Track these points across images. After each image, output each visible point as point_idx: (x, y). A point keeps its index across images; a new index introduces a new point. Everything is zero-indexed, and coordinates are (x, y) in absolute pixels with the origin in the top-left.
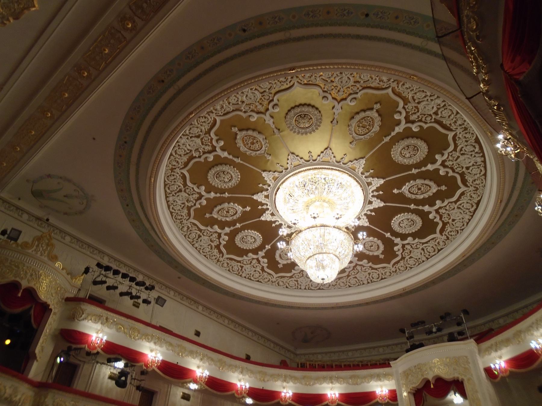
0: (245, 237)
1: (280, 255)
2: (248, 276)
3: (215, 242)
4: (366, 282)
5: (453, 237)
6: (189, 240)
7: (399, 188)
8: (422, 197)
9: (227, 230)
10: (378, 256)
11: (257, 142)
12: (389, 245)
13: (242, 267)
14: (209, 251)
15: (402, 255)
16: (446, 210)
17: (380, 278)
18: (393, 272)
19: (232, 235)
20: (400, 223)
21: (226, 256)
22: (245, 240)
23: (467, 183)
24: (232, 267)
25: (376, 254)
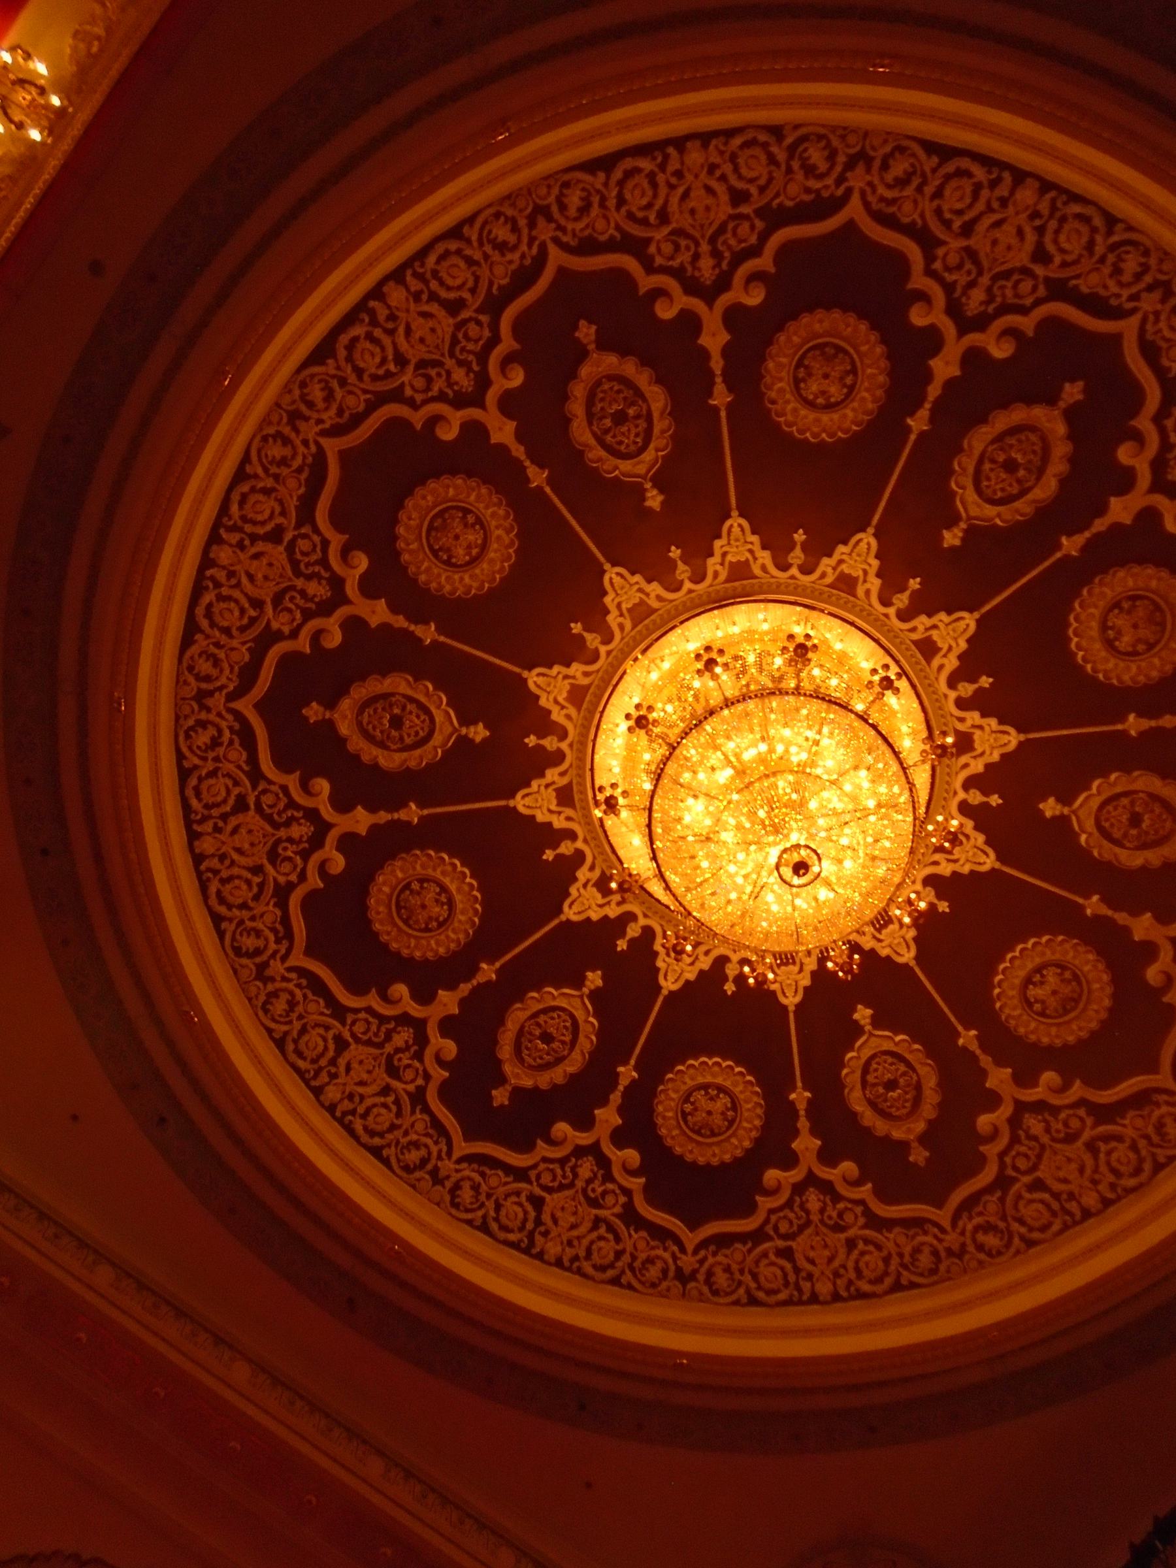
0: (415, 886)
2: (347, 1105)
3: (286, 867)
4: (824, 1288)
6: (194, 803)
7: (1066, 799)
9: (361, 820)
10: (904, 1146)
11: (638, 417)
12: (963, 1090)
14: (244, 906)
15: (1002, 1166)
17: (888, 1281)
18: (950, 1252)
19: (369, 854)
21: (298, 959)
22: (415, 901)
24: (303, 1031)
25: (897, 1134)
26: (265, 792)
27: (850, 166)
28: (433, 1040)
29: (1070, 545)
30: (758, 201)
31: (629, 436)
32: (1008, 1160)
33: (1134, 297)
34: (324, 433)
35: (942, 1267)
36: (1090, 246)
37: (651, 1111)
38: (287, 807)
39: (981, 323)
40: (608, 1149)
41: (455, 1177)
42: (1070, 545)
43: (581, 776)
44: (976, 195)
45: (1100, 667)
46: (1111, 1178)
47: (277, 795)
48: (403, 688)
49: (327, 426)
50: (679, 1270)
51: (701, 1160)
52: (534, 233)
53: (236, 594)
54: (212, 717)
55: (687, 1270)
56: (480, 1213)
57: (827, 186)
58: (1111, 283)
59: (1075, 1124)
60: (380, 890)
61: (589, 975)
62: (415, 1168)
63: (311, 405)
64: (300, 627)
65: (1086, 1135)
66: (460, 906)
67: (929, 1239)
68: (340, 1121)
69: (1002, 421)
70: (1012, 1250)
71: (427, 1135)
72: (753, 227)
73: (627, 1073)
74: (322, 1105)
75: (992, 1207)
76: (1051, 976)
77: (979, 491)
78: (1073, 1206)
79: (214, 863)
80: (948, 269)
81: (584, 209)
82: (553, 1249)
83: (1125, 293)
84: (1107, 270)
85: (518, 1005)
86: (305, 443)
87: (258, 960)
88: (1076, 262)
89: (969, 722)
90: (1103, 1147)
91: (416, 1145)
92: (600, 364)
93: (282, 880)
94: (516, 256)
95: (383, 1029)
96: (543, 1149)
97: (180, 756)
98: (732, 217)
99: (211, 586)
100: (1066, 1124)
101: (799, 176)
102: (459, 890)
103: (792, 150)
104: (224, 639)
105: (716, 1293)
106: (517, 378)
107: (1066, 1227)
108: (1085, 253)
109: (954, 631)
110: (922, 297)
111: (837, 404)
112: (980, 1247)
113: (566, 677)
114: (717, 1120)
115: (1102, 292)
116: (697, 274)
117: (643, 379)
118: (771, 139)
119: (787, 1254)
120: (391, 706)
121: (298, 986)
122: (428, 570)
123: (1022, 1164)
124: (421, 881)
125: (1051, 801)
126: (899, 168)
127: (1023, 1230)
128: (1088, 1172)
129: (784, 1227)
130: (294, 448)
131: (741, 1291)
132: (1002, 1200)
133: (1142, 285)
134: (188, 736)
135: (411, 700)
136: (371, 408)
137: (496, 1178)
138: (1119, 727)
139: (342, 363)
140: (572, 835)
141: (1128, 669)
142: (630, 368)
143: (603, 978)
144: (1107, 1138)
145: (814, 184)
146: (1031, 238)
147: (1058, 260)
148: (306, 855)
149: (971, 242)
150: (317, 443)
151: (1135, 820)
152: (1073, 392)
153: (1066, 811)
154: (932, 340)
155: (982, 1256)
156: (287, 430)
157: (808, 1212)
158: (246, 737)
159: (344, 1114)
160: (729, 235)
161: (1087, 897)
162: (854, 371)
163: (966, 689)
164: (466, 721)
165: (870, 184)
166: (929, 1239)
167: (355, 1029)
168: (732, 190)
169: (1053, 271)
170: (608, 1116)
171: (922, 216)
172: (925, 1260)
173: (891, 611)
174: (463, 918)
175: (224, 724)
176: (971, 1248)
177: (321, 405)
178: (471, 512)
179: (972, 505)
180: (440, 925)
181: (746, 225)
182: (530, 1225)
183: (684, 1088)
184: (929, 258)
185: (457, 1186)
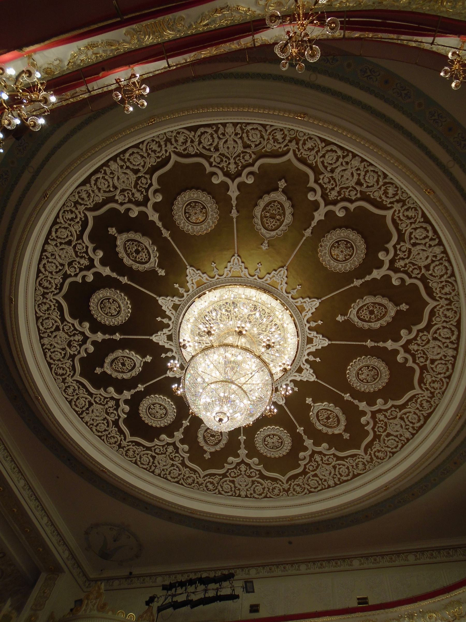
1: (116, 358)
2: (48, 347)
3: (73, 270)
4: (157, 471)
5: (294, 493)
7: (314, 402)
8: (320, 428)
9: (106, 271)
10: (206, 452)
11: (278, 220)
13: (57, 329)
15: (227, 472)
16: (322, 460)
17: (176, 480)
18: (198, 483)
20: (269, 436)
23: (369, 449)
25: (205, 448)
26: (80, 244)
27: (398, 201)
28: (87, 344)
29: (369, 343)
30: (364, 188)
31: (271, 223)
32: (230, 471)
33: (441, 298)
34: (174, 152)
35: (193, 485)
36: (442, 276)
37: (141, 401)
38: (84, 252)
39: (396, 271)
40: (121, 403)
41: (70, 384)
42: (369, 343)
43: (185, 306)
44: (424, 238)
45: (350, 378)
46: (252, 492)
47: (83, 247)
48: (147, 244)
49: (177, 151)
50: (120, 444)
51: (146, 422)
52: (289, 144)
53: (110, 180)
54: (77, 212)
55: (122, 445)
56: (71, 398)
57: (387, 202)
58: (438, 289)
59: (253, 474)
60: (99, 295)
61: (148, 356)
62: (59, 375)
63: (176, 141)
64: (125, 203)
65: (254, 479)
66: (122, 314)
67: (195, 476)
68: (43, 350)
69: (379, 299)
70: (214, 492)
71: (69, 368)
72: (356, 194)
73: (141, 387)
74: (41, 342)
75: (217, 479)
76: (275, 439)
77: (358, 312)
78: (238, 492)
79: (49, 255)
80: (400, 250)
81: (311, 150)
82: (87, 419)
84: (440, 285)
85: (121, 351)
86: (166, 151)
87: (46, 291)
88: (434, 276)
89: (305, 367)
90: (256, 484)
91: (64, 369)
92: (278, 196)
93: (68, 272)
94: (278, 146)
95: (74, 332)
96: (102, 391)
97: (57, 216)
98: (353, 187)
99: (103, 172)
100: (251, 473)
101: (381, 192)
102: (124, 310)
103: (385, 184)
104: (96, 191)
105: (127, 455)
106: (250, 181)
107: (232, 495)
109: (321, 342)
110: (387, 251)
111: (339, 261)
112: (206, 486)
113: (200, 276)
114: (158, 415)
115: (434, 289)
116: (329, 194)
117: (289, 210)
118: (382, 176)
119: (154, 458)
120: (139, 246)
121: (54, 305)
122: (179, 216)
123: (233, 474)
124: (114, 300)
125: (311, 399)
126: (410, 213)
127: (221, 489)
128: (248, 487)
129: (157, 451)
130: (161, 150)
131: (134, 459)
132: (221, 479)
133: (445, 297)
134: (64, 212)
135: (147, 249)
136: (196, 155)
137: (82, 391)
138: (343, 395)
139: (196, 136)
140: (170, 319)
141: (357, 383)
142: (287, 204)
143: (152, 360)
144: (258, 482)
145: (383, 197)
146: (429, 261)
147: (430, 272)
148: (81, 270)
149: (413, 249)
150: (170, 153)
151: (328, 418)
152: (404, 307)
153: (312, 404)
154: (380, 265)
155: (205, 489)
156: (162, 143)
157: (167, 451)
158: (85, 224)
159: (46, 348)
160: (348, 191)
161: (300, 427)
162: (351, 256)
163: (311, 358)
164: (160, 266)
165: (399, 211)
166: (195, 476)
167: (65, 327)
168: (359, 180)
169: (427, 274)
170: (127, 395)
171: (406, 230)
172: (190, 481)
173: (308, 325)
174: (120, 318)
175: (79, 216)
176: (204, 485)
177: (180, 143)
178: (205, 208)
179: (352, 314)
180: (111, 316)
181: (355, 192)
182: (84, 409)
183: (154, 401)
184: (398, 243)
185: (69, 387)
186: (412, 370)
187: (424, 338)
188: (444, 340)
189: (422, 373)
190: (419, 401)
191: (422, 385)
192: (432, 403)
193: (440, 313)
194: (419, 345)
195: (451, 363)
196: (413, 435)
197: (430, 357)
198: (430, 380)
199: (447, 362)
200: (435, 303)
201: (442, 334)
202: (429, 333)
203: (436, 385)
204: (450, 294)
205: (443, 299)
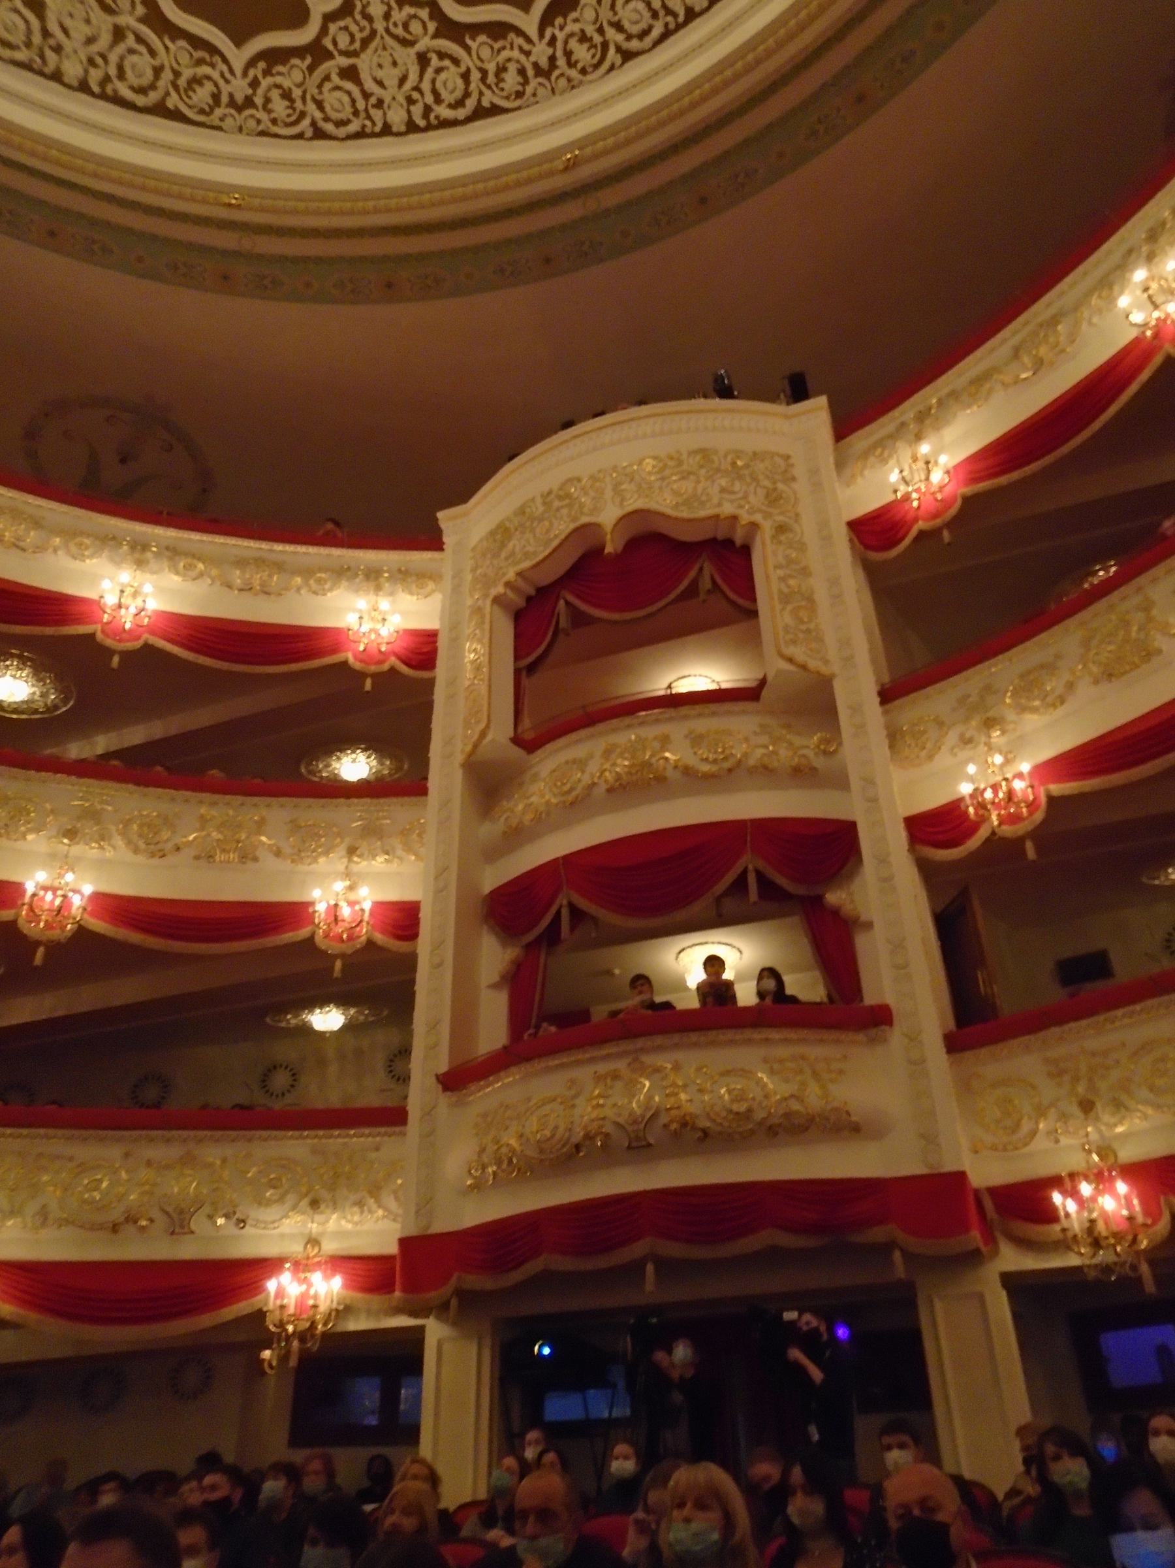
33: (553, 41)
36: (618, 26)
58: (576, 28)
83: (560, 36)
84: (590, 30)
108: (616, 19)
115: (574, 15)
133: (559, 53)
186: (300, 17)
187: (415, 27)
188: (426, 86)
189: (298, 52)
190: (205, 70)
191: (262, 65)
192: (218, 112)
193: (506, 54)
194: (387, 16)
195: (364, 126)
196: (83, 87)
197: (364, 63)
198: (286, 83)
199: (363, 115)
200: (532, 31)
201: (443, 76)
202: (436, 35)
203: (279, 107)
204: (571, 64)
205: (550, 51)
